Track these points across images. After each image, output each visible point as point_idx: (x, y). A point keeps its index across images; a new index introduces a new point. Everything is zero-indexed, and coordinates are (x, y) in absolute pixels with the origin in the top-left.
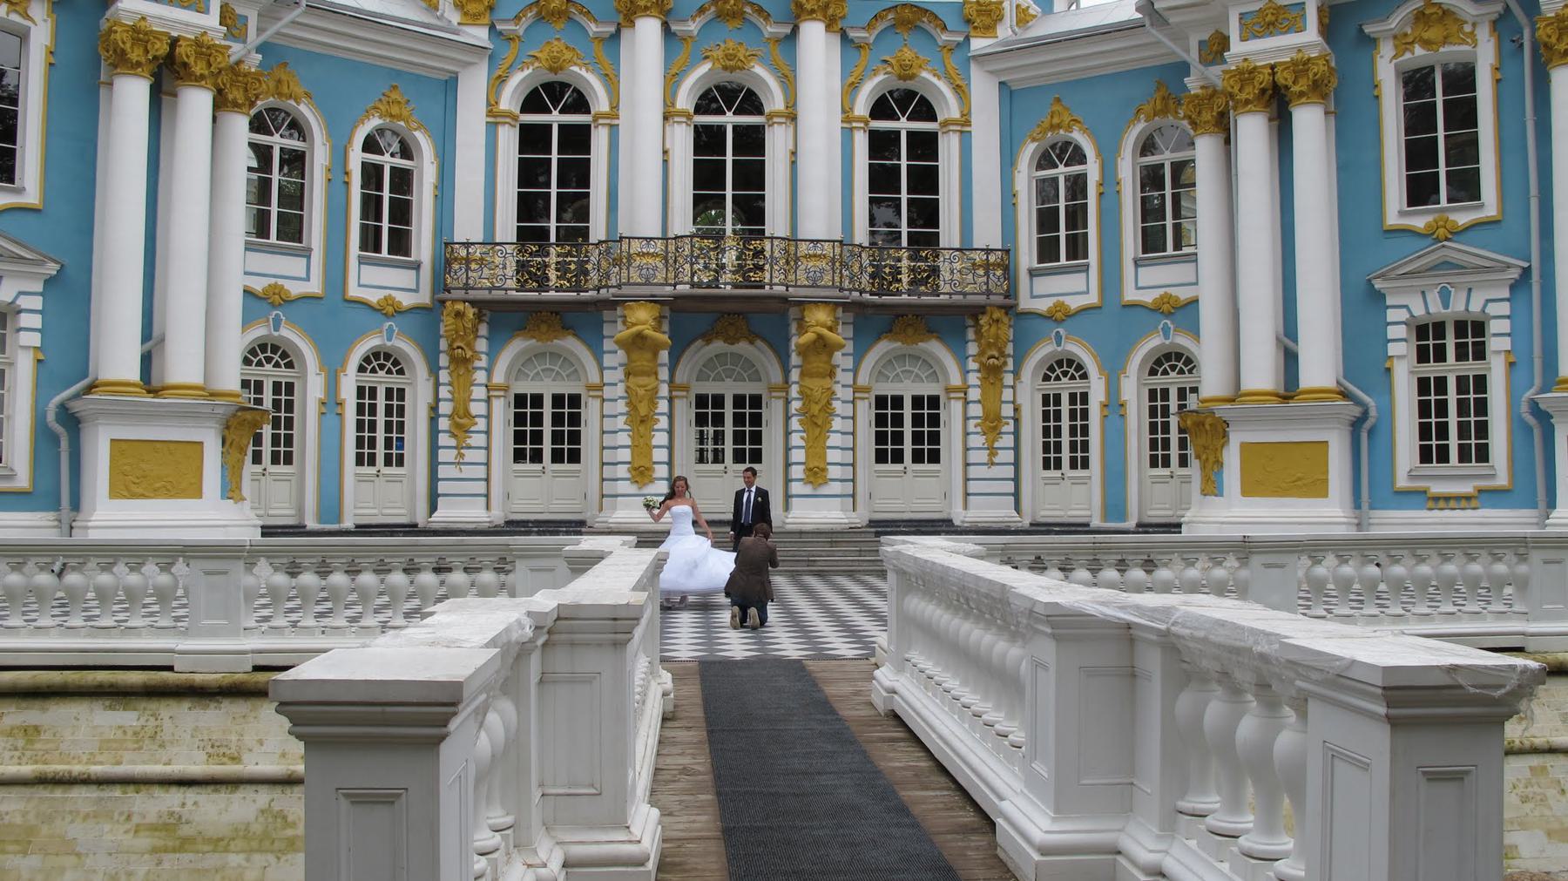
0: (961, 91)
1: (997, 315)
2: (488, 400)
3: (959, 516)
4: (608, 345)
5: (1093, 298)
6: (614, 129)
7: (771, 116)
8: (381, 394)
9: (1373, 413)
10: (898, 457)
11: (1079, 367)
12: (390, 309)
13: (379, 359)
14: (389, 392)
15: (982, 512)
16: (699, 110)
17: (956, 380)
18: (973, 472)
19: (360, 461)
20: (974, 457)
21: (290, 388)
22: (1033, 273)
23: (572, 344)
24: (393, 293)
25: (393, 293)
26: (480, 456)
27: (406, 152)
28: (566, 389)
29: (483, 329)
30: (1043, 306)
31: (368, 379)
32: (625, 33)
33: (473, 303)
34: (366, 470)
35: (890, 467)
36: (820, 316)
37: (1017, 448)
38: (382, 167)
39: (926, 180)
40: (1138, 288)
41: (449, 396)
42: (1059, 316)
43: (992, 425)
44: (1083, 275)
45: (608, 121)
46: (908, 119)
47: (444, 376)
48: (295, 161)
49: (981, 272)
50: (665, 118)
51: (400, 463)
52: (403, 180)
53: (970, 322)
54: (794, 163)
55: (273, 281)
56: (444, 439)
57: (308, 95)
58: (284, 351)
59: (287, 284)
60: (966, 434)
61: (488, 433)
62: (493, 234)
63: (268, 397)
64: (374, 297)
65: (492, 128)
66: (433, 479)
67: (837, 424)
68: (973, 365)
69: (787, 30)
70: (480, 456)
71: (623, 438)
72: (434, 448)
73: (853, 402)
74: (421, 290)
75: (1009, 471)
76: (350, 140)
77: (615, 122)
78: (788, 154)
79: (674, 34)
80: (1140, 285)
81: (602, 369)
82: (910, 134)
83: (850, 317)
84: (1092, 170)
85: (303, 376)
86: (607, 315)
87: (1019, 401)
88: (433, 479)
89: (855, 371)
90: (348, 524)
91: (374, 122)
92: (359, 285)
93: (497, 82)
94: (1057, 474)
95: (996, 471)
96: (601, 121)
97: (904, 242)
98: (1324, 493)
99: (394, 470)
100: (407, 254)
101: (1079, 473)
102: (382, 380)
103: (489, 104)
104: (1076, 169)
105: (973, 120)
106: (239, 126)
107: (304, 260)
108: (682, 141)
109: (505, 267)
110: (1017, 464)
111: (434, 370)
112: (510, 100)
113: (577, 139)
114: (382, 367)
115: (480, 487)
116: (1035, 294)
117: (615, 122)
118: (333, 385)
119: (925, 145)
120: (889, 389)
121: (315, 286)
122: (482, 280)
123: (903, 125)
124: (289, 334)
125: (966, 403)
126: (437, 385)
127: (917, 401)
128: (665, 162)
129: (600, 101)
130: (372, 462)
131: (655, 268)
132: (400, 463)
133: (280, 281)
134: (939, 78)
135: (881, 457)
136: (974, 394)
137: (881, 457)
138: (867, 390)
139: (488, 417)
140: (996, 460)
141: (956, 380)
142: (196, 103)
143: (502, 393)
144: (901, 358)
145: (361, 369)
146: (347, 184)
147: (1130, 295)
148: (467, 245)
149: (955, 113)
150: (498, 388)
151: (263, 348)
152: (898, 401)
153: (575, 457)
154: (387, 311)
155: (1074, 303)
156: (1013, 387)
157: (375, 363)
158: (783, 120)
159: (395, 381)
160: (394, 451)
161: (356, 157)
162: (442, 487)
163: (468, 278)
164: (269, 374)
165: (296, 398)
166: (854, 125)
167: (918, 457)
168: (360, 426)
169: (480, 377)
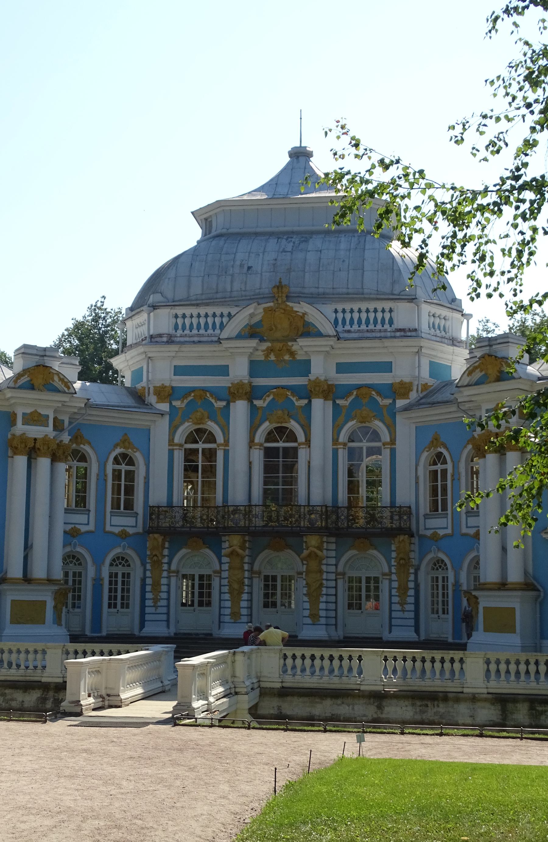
0: (392, 428)
2: (169, 578)
3: (387, 636)
4: (223, 552)
5: (449, 531)
6: (226, 453)
7: (299, 444)
8: (120, 576)
9: (542, 594)
11: (446, 565)
12: (124, 536)
13: (121, 560)
14: (123, 574)
15: (397, 634)
16: (267, 440)
17: (386, 570)
18: (394, 614)
19: (110, 606)
20: (394, 607)
21: (80, 574)
22: (426, 516)
23: (208, 551)
24: (125, 528)
25: (125, 528)
26: (164, 603)
27: (131, 462)
28: (206, 572)
29: (167, 545)
30: (429, 533)
31: (114, 570)
32: (232, 404)
33: (161, 533)
34: (113, 610)
36: (313, 541)
37: (417, 603)
40: (467, 527)
41: (150, 575)
42: (435, 538)
43: (403, 590)
44: (446, 519)
45: (223, 447)
47: (148, 567)
49: (396, 517)
50: (250, 447)
51: (128, 607)
52: (130, 476)
53: (393, 542)
54: (309, 466)
55: (73, 526)
56: (149, 595)
57: (89, 444)
60: (391, 596)
61: (168, 592)
62: (172, 502)
63: (71, 579)
64: (116, 530)
65: (171, 453)
66: (143, 613)
67: (324, 591)
68: (393, 563)
69: (306, 401)
70: (164, 603)
71: (227, 596)
72: (143, 599)
73: (336, 580)
74: (138, 526)
75: (412, 615)
77: (227, 448)
78: (307, 463)
79: (255, 405)
80: (469, 525)
81: (221, 563)
83: (333, 539)
84: (449, 467)
85: (86, 569)
86: (223, 538)
87: (419, 581)
88: (143, 613)
89: (336, 565)
90: (104, 633)
91: (118, 451)
92: (111, 525)
93: (173, 429)
94: (436, 616)
95: (406, 615)
96: (220, 447)
98: (514, 632)
99: (125, 610)
100: (133, 510)
101: (445, 616)
102: (120, 570)
103: (169, 440)
104: (444, 467)
105: (397, 442)
107: (87, 516)
108: (258, 456)
109: (175, 518)
110: (417, 611)
111: (144, 564)
112: (180, 437)
113: (210, 455)
114: (120, 563)
115: (164, 617)
116: (427, 527)
117: (227, 448)
118: (99, 571)
120: (354, 574)
121: (91, 527)
122: (165, 523)
124: (79, 549)
125: (391, 581)
126: (145, 570)
127: (368, 579)
128: (250, 468)
129: (220, 439)
130: (115, 607)
131: (240, 520)
132: (128, 607)
136: (394, 577)
138: (344, 574)
139: (169, 585)
141: (386, 570)
143: (175, 574)
145: (111, 565)
146: (106, 480)
147: (464, 530)
148: (158, 507)
149: (388, 439)
150: (173, 572)
151: (69, 557)
153: (209, 604)
154: (124, 535)
155: (441, 532)
156: (416, 574)
157: (117, 562)
158: (304, 446)
159: (126, 570)
160: (125, 602)
161: (110, 467)
162: (147, 617)
163: (158, 522)
164: (73, 568)
165: (83, 579)
166: (339, 447)
168: (110, 590)
169: (165, 567)
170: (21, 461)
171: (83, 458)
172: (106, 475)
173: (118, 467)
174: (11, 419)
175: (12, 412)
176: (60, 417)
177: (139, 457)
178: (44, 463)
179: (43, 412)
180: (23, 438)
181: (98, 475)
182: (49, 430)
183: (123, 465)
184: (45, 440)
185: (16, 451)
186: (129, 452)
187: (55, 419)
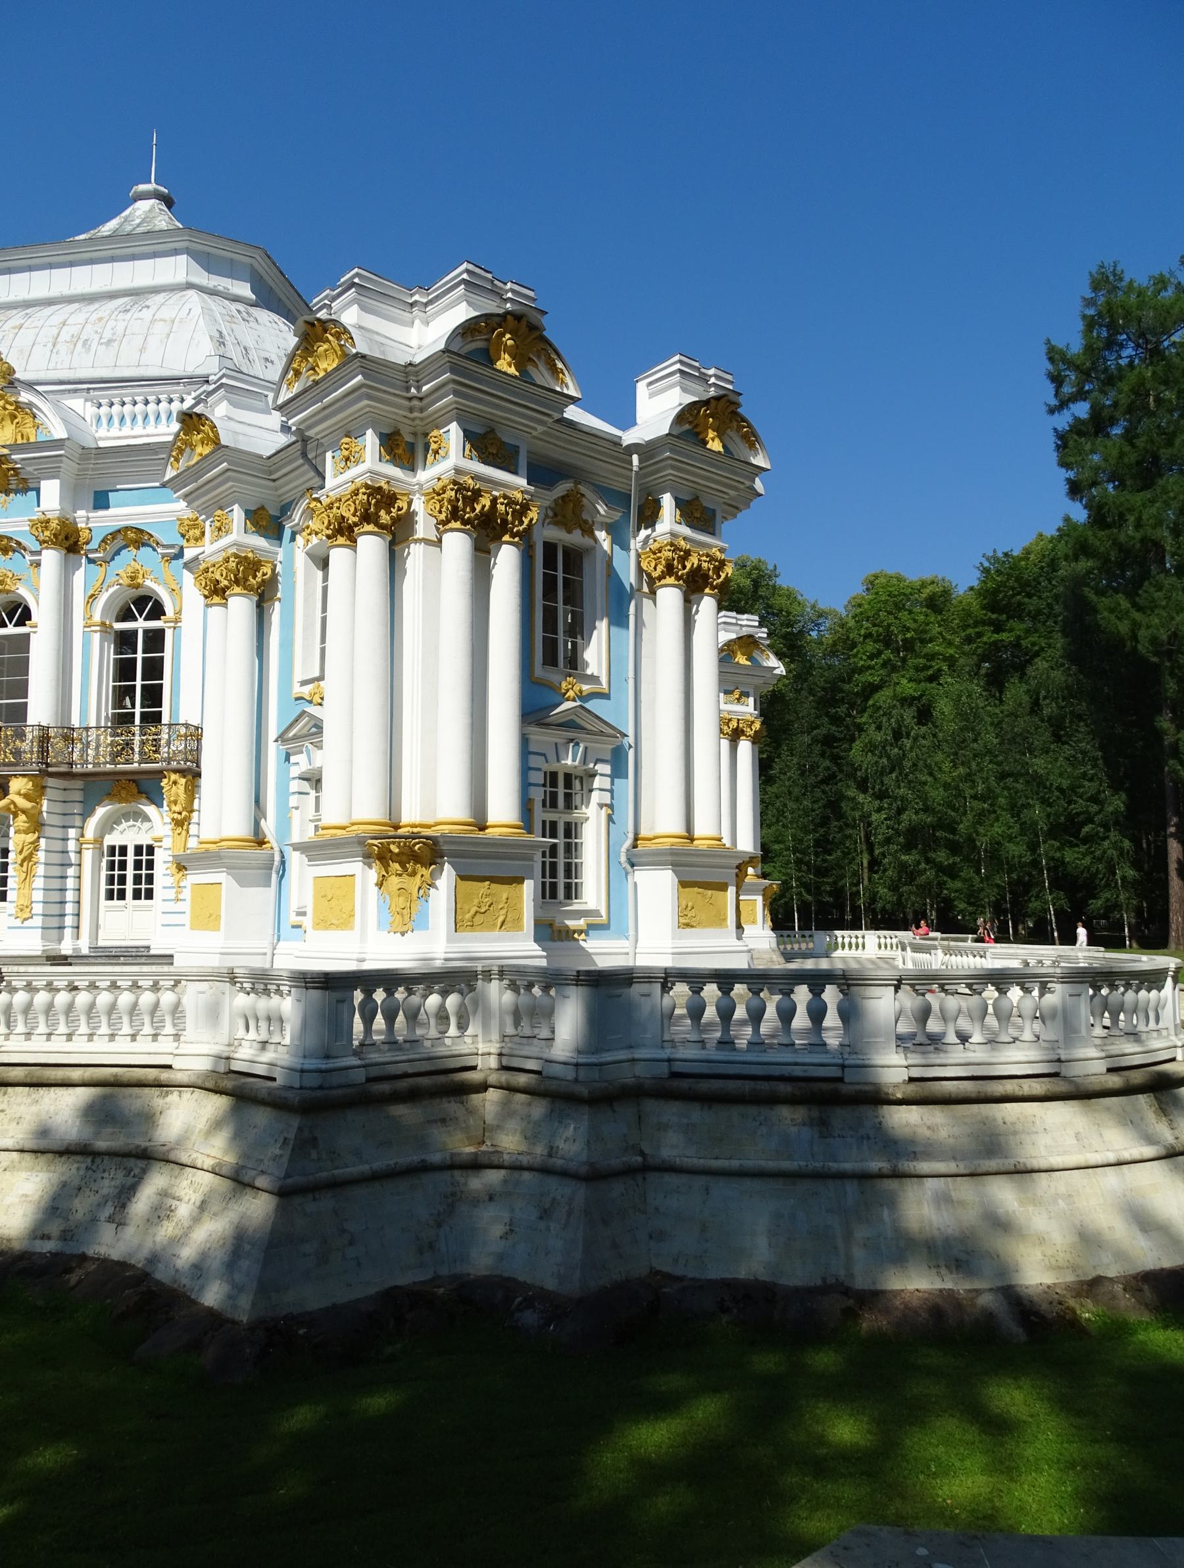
1: (174, 777)
10: (122, 895)
35: (116, 902)
39: (154, 669)
46: (146, 619)
82: (146, 632)
97: (137, 721)
119: (155, 640)
123: (141, 625)
127: (138, 850)
134: (159, 584)
135: (110, 895)
137: (110, 895)
140: (180, 897)
144: (126, 816)
152: (123, 850)
166: (93, 628)
167: (137, 895)
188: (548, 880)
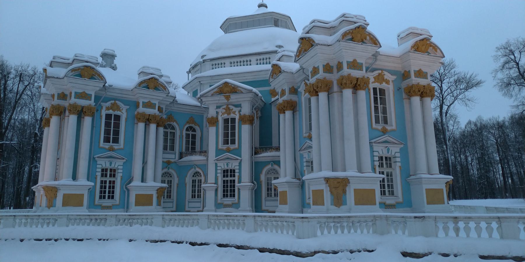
27: (194, 130)
38: (189, 134)
48: (173, 134)
52: (194, 137)
55: (168, 160)
58: (170, 174)
59: (171, 160)
76: (183, 129)
106: (161, 130)
107: (174, 155)
124: (171, 171)
133: (170, 160)
142: (153, 127)
161: (184, 132)
170: (141, 126)
171: (173, 128)
172: (182, 136)
173: (188, 132)
174: (137, 105)
175: (137, 101)
176: (161, 106)
177: (197, 128)
178: (153, 127)
179: (153, 102)
180: (143, 115)
181: (180, 136)
182: (155, 111)
183: (191, 132)
184: (154, 116)
185: (139, 120)
186: (193, 125)
187: (159, 107)
188: (382, 190)
